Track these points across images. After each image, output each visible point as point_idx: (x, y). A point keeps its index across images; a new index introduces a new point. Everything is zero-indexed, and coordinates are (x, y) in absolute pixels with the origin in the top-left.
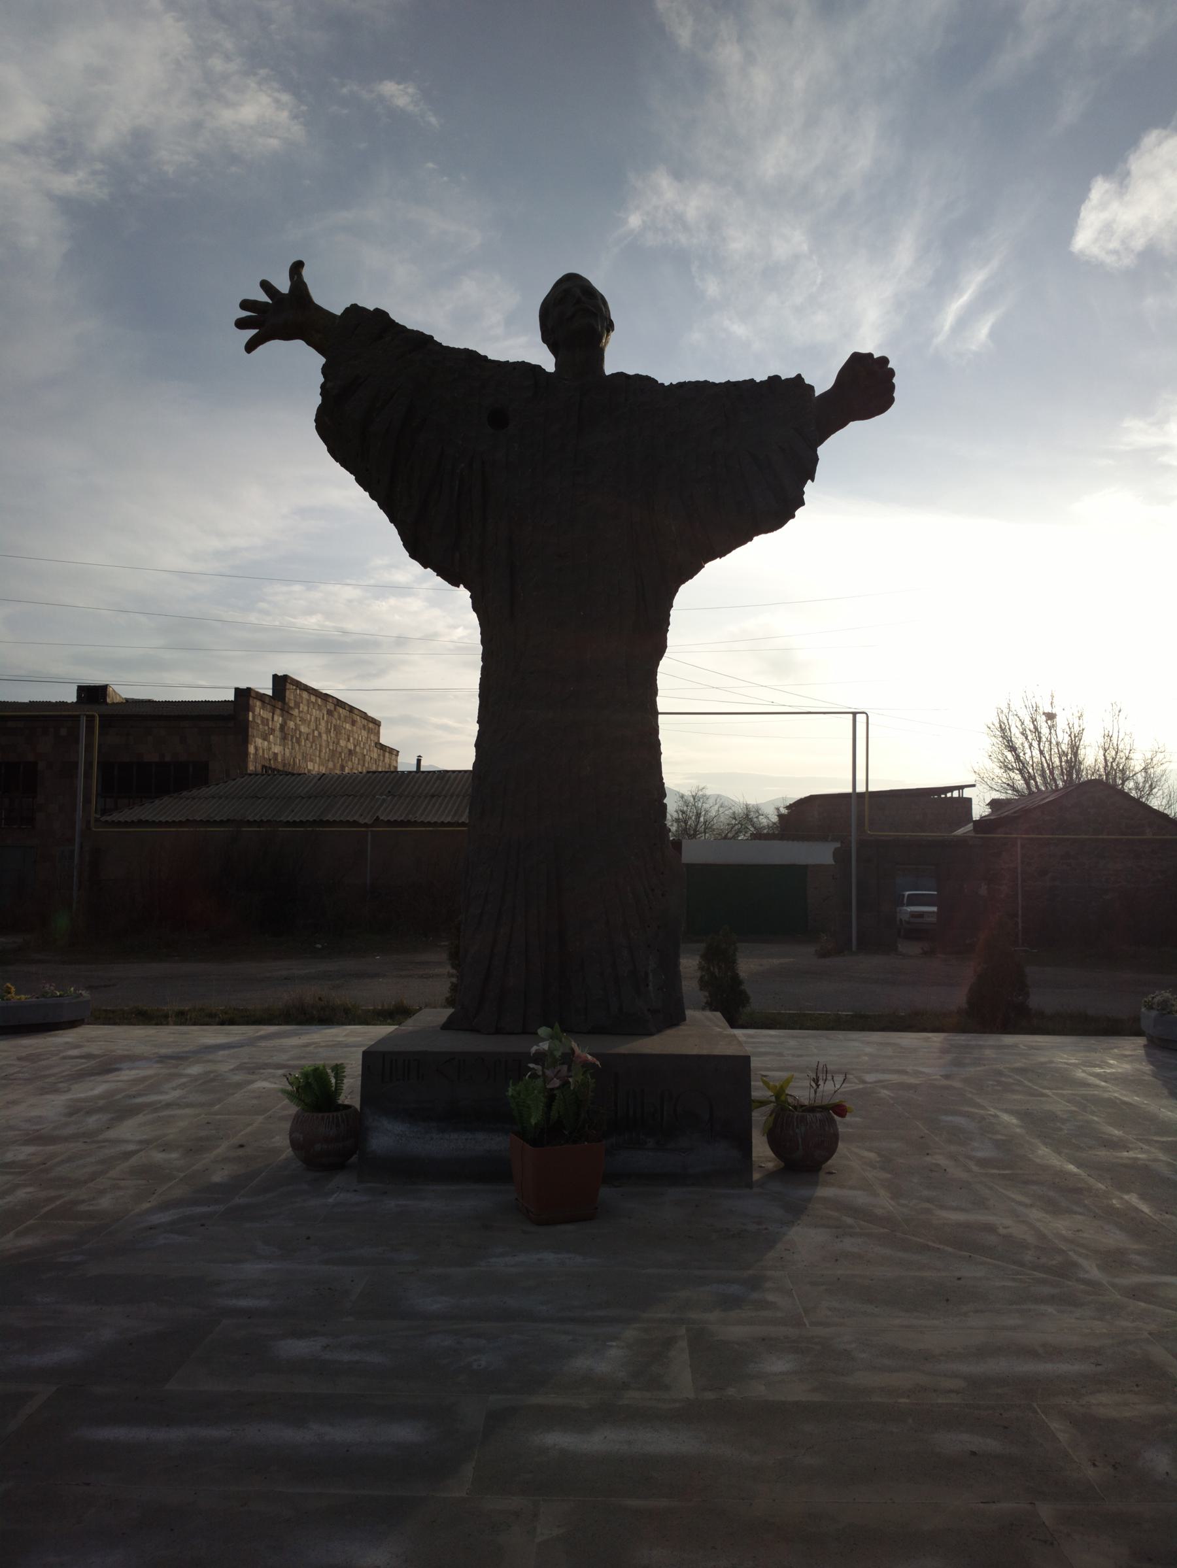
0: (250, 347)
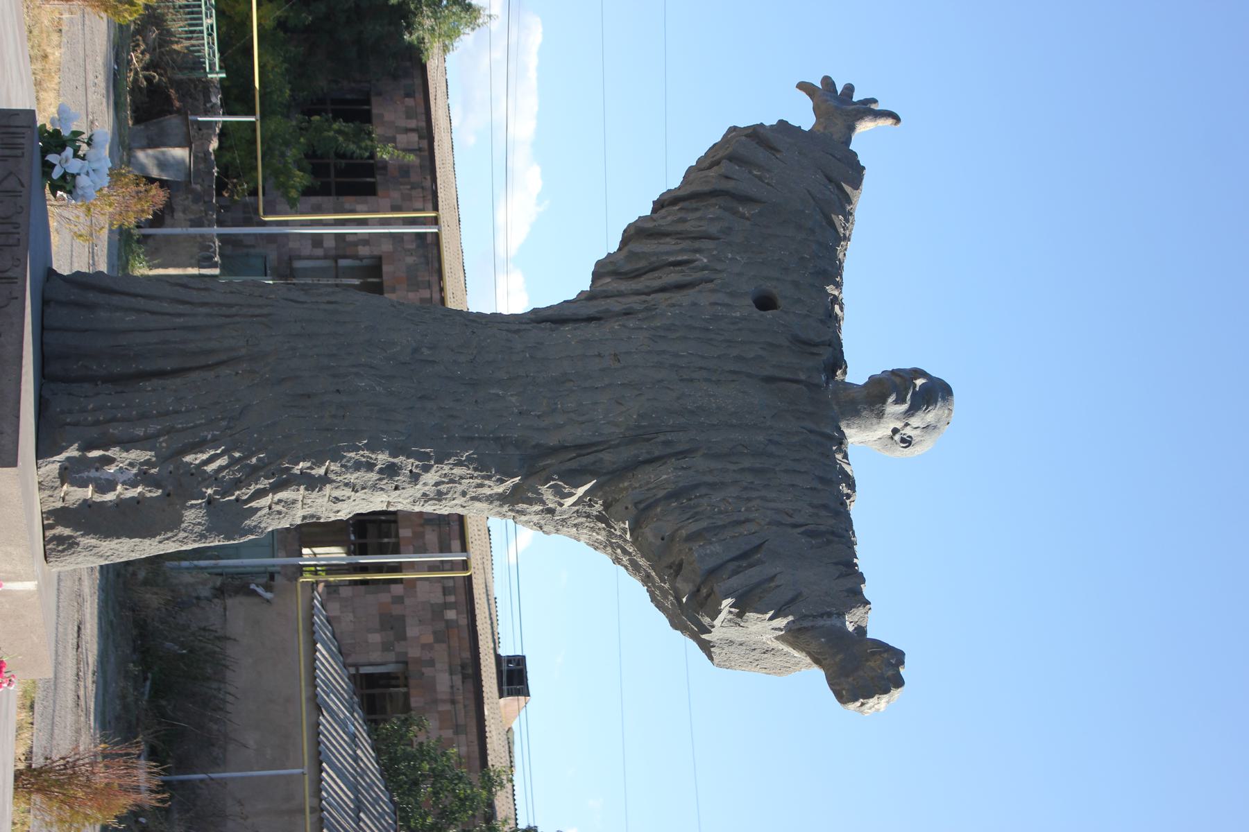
0: (803, 86)
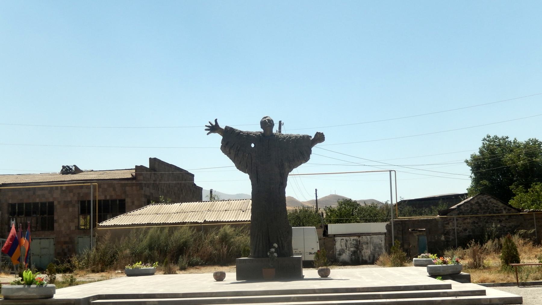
0: (208, 134)
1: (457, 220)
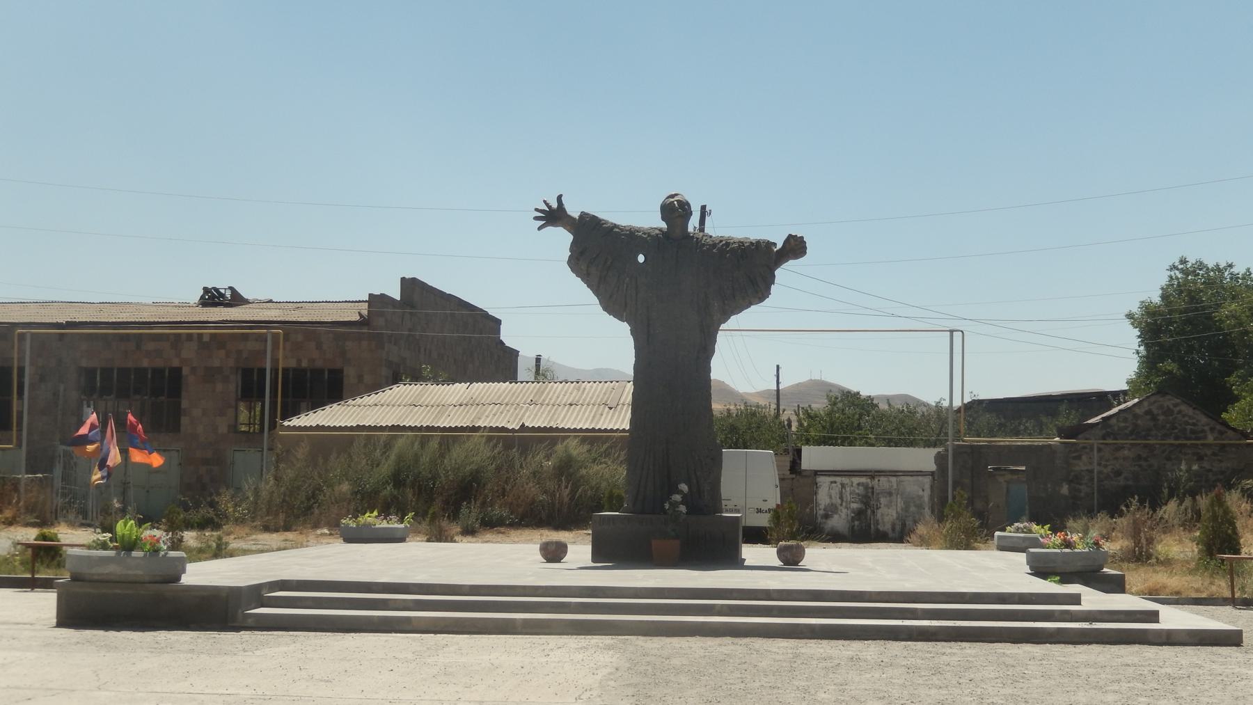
0: (539, 229)
1: (1099, 450)
